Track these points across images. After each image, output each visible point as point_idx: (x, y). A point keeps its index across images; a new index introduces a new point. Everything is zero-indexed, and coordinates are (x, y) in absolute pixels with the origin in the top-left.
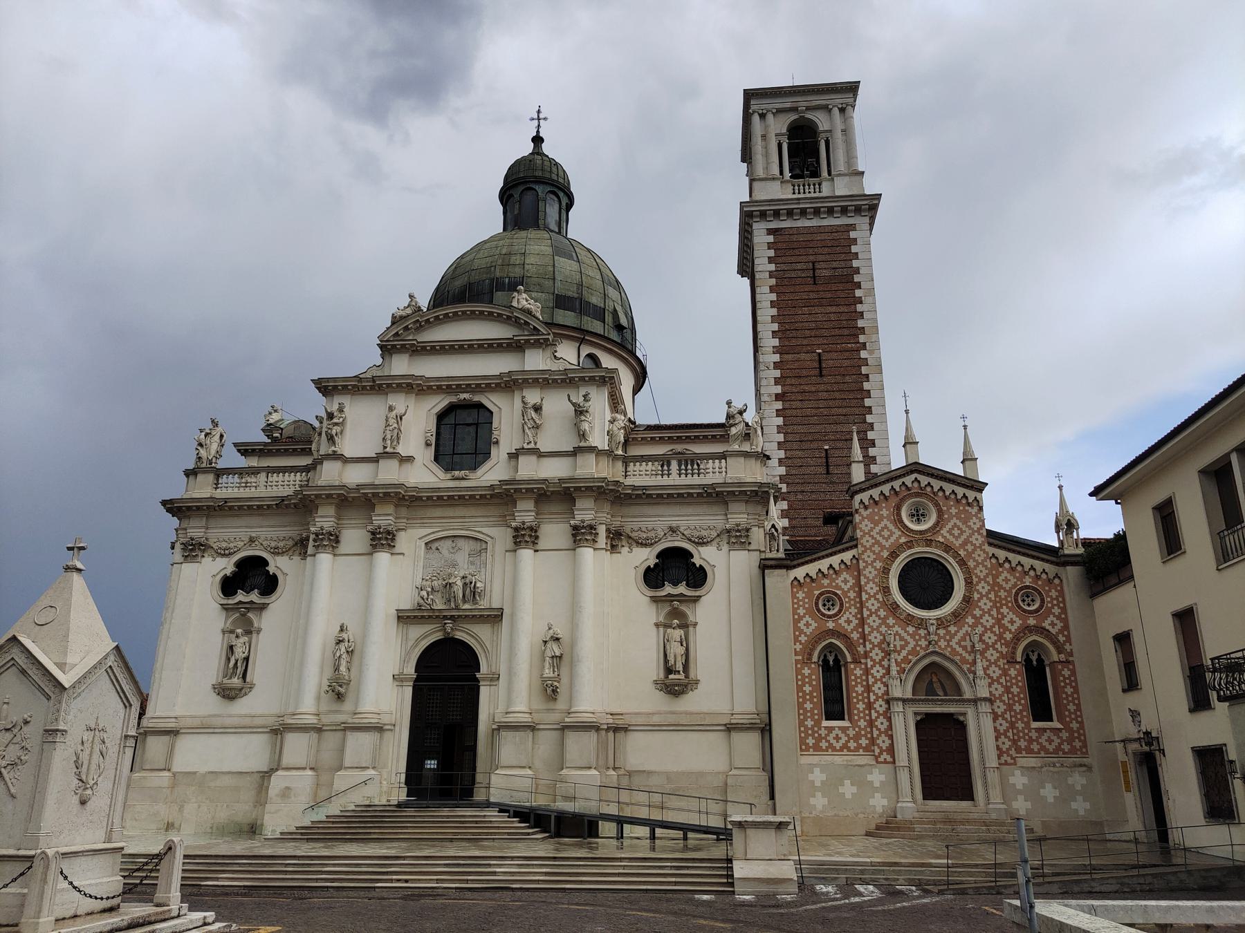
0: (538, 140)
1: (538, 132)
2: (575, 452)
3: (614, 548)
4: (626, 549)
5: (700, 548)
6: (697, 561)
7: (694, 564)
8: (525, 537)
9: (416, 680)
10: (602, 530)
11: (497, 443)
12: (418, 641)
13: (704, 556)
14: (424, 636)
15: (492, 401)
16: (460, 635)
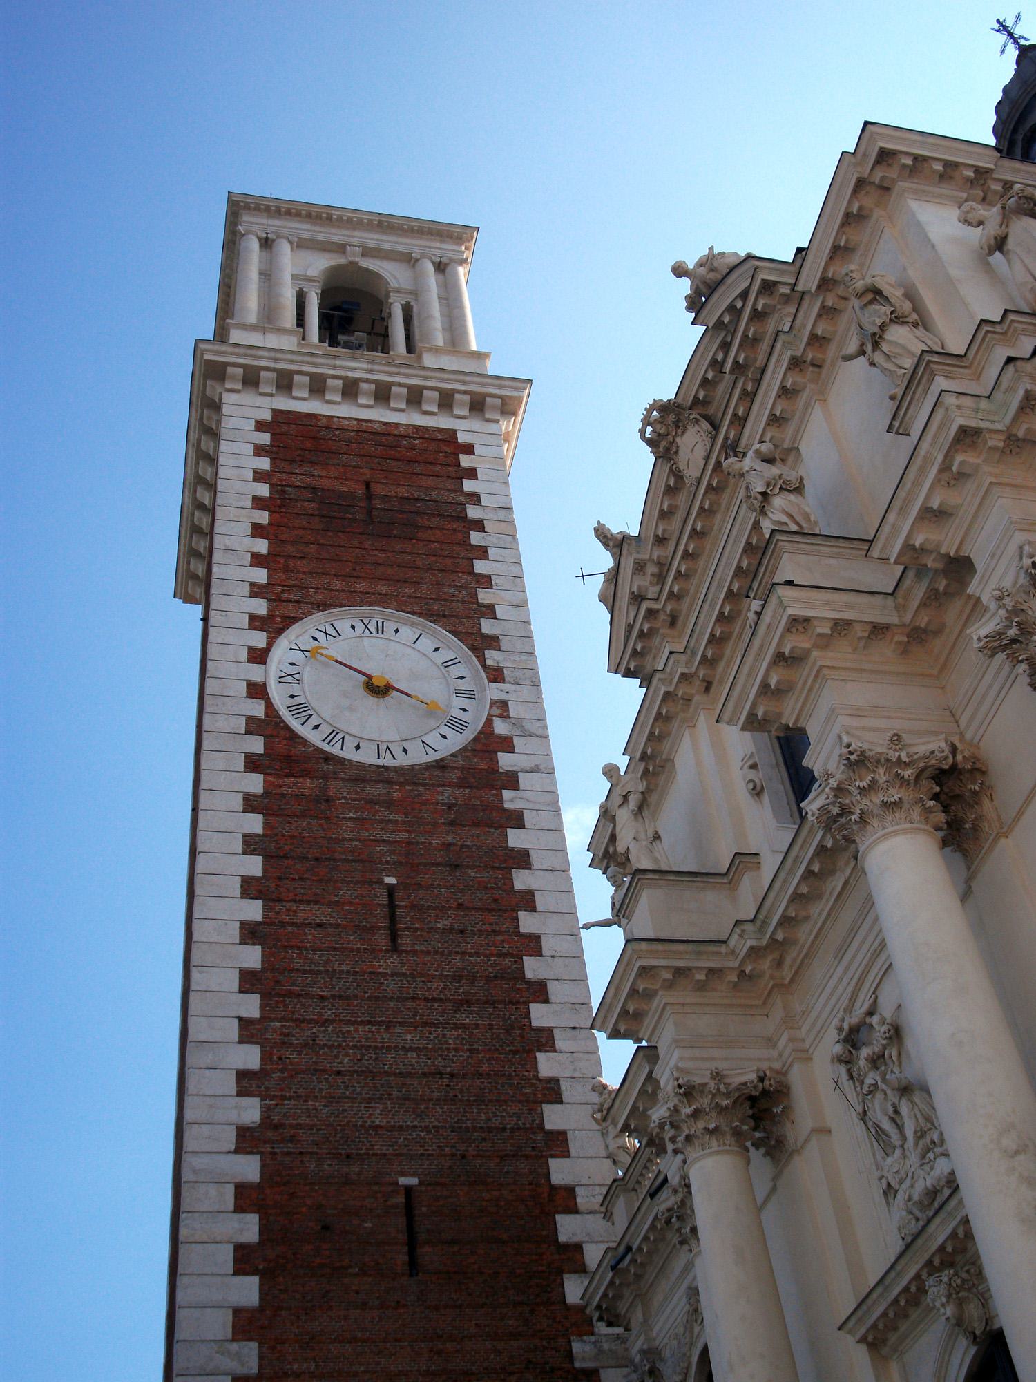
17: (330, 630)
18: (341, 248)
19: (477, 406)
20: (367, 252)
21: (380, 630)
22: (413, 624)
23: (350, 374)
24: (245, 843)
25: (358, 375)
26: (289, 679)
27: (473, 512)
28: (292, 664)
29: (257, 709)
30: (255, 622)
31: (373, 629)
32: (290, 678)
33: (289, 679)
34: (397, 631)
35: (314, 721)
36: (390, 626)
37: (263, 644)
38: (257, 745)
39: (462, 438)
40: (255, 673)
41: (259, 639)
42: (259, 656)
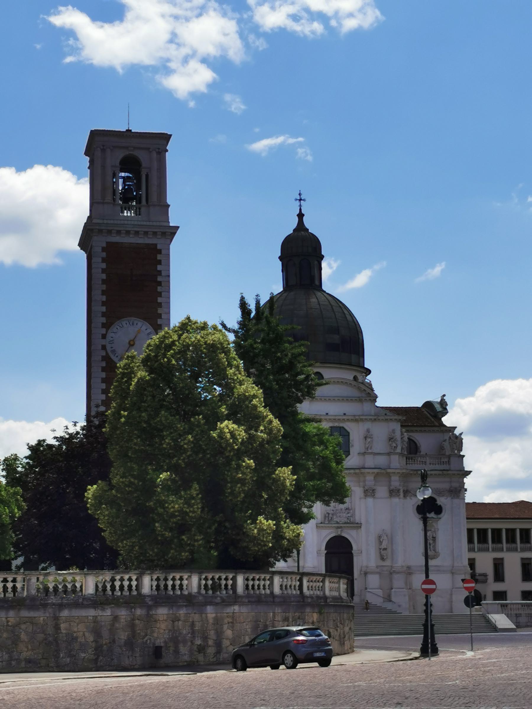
0: (301, 216)
1: (300, 210)
2: (389, 454)
3: (405, 496)
4: (408, 498)
5: (440, 498)
6: (439, 503)
7: (437, 504)
8: (369, 493)
9: (326, 554)
10: (401, 491)
11: (353, 446)
12: (326, 537)
13: (441, 501)
14: (328, 534)
15: (349, 426)
16: (344, 535)
17: (121, 326)
18: (127, 148)
19: (164, 234)
20: (135, 148)
21: (133, 324)
22: (141, 322)
23: (128, 229)
24: (102, 391)
25: (130, 229)
26: (111, 342)
27: (159, 279)
28: (112, 337)
29: (104, 353)
30: (104, 325)
31: (131, 324)
32: (111, 342)
33: (111, 342)
34: (137, 324)
35: (116, 355)
36: (135, 322)
37: (105, 333)
38: (104, 364)
39: (159, 247)
40: (103, 342)
41: (104, 331)
42: (104, 336)
